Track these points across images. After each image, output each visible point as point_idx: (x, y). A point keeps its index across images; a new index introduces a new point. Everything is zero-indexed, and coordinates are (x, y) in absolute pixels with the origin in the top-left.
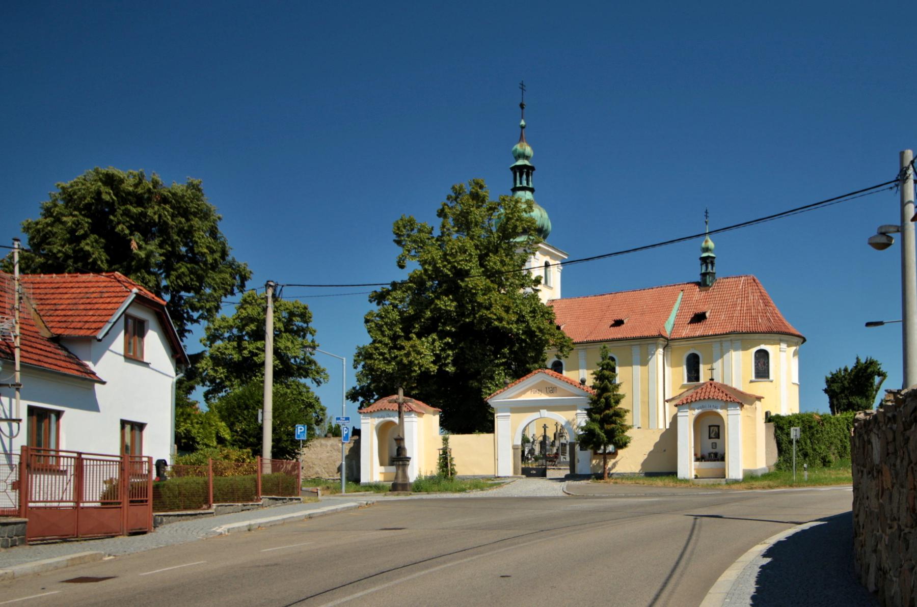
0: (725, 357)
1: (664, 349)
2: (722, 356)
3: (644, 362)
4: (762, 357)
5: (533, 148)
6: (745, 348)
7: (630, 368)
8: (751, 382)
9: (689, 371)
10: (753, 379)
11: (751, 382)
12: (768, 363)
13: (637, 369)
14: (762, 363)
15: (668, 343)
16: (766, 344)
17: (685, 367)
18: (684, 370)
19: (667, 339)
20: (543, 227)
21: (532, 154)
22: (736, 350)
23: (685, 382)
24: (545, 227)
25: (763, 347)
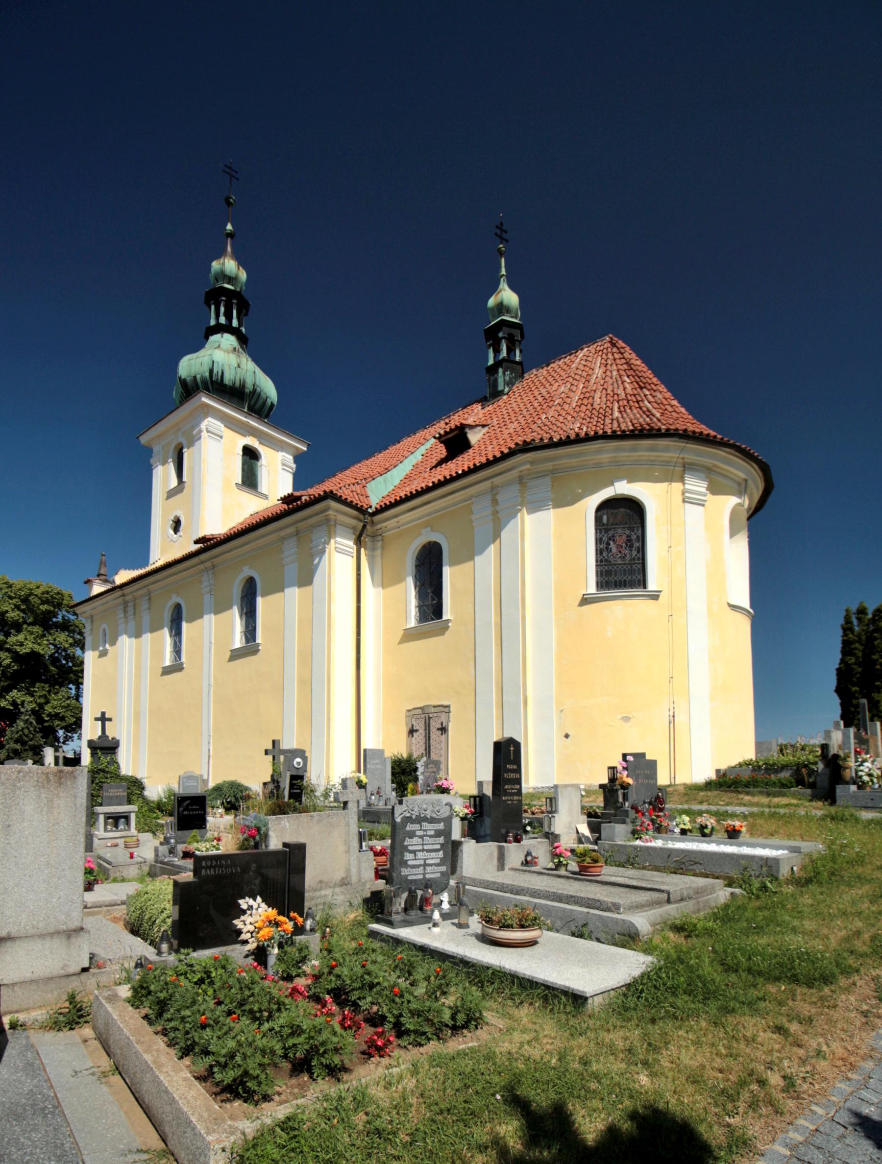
0: (504, 534)
1: (359, 542)
2: (496, 535)
3: (306, 578)
4: (623, 522)
5: (241, 263)
6: (565, 499)
7: (278, 596)
8: (586, 601)
9: (421, 595)
10: (592, 589)
11: (586, 601)
12: (643, 539)
13: (293, 594)
14: (622, 540)
15: (367, 524)
16: (632, 479)
17: (410, 582)
18: (408, 592)
19: (361, 510)
20: (243, 386)
21: (243, 276)
22: (535, 507)
23: (412, 623)
24: (249, 387)
25: (623, 488)
